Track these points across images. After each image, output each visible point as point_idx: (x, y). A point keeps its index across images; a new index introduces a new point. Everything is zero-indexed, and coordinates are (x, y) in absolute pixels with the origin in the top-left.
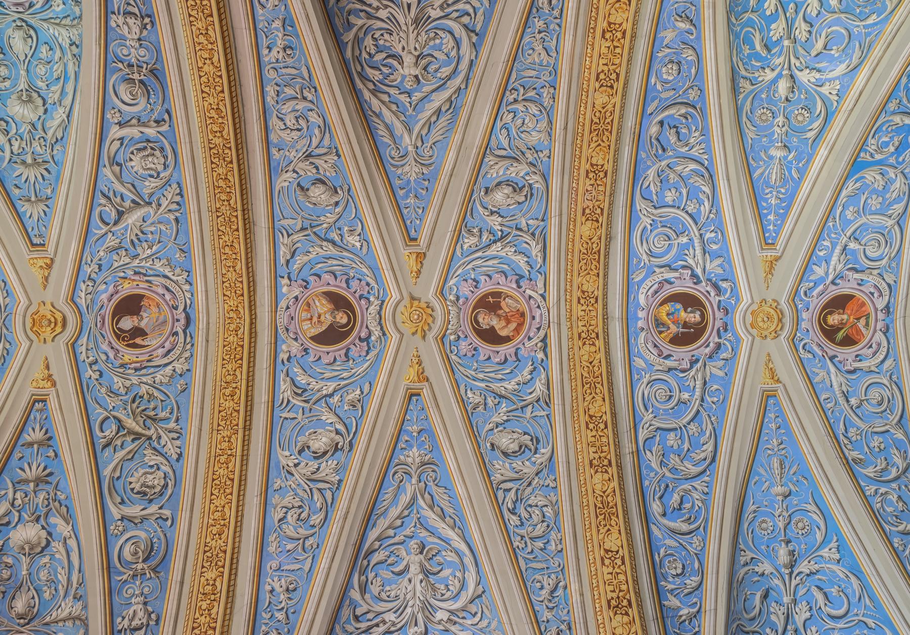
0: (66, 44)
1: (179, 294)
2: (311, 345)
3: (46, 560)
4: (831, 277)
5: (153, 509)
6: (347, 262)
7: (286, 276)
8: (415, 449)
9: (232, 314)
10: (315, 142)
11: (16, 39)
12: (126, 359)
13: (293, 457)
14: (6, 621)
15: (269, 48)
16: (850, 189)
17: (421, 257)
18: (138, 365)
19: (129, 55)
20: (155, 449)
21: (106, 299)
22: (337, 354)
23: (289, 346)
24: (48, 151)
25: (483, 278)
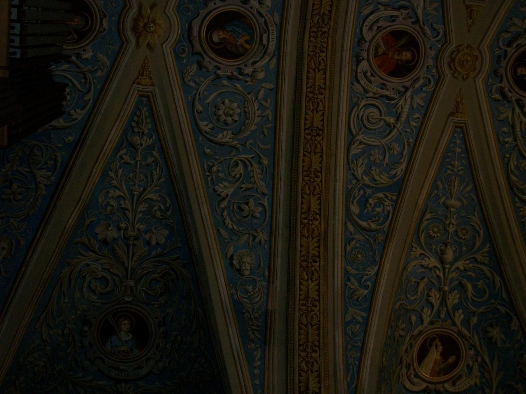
4: (409, 94)
16: (399, 169)
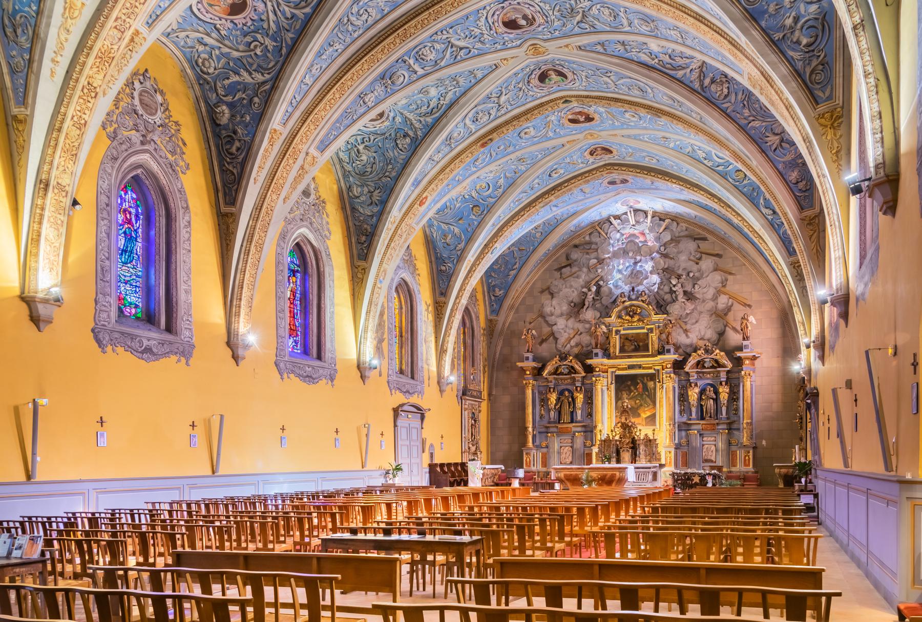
1: (494, 9)
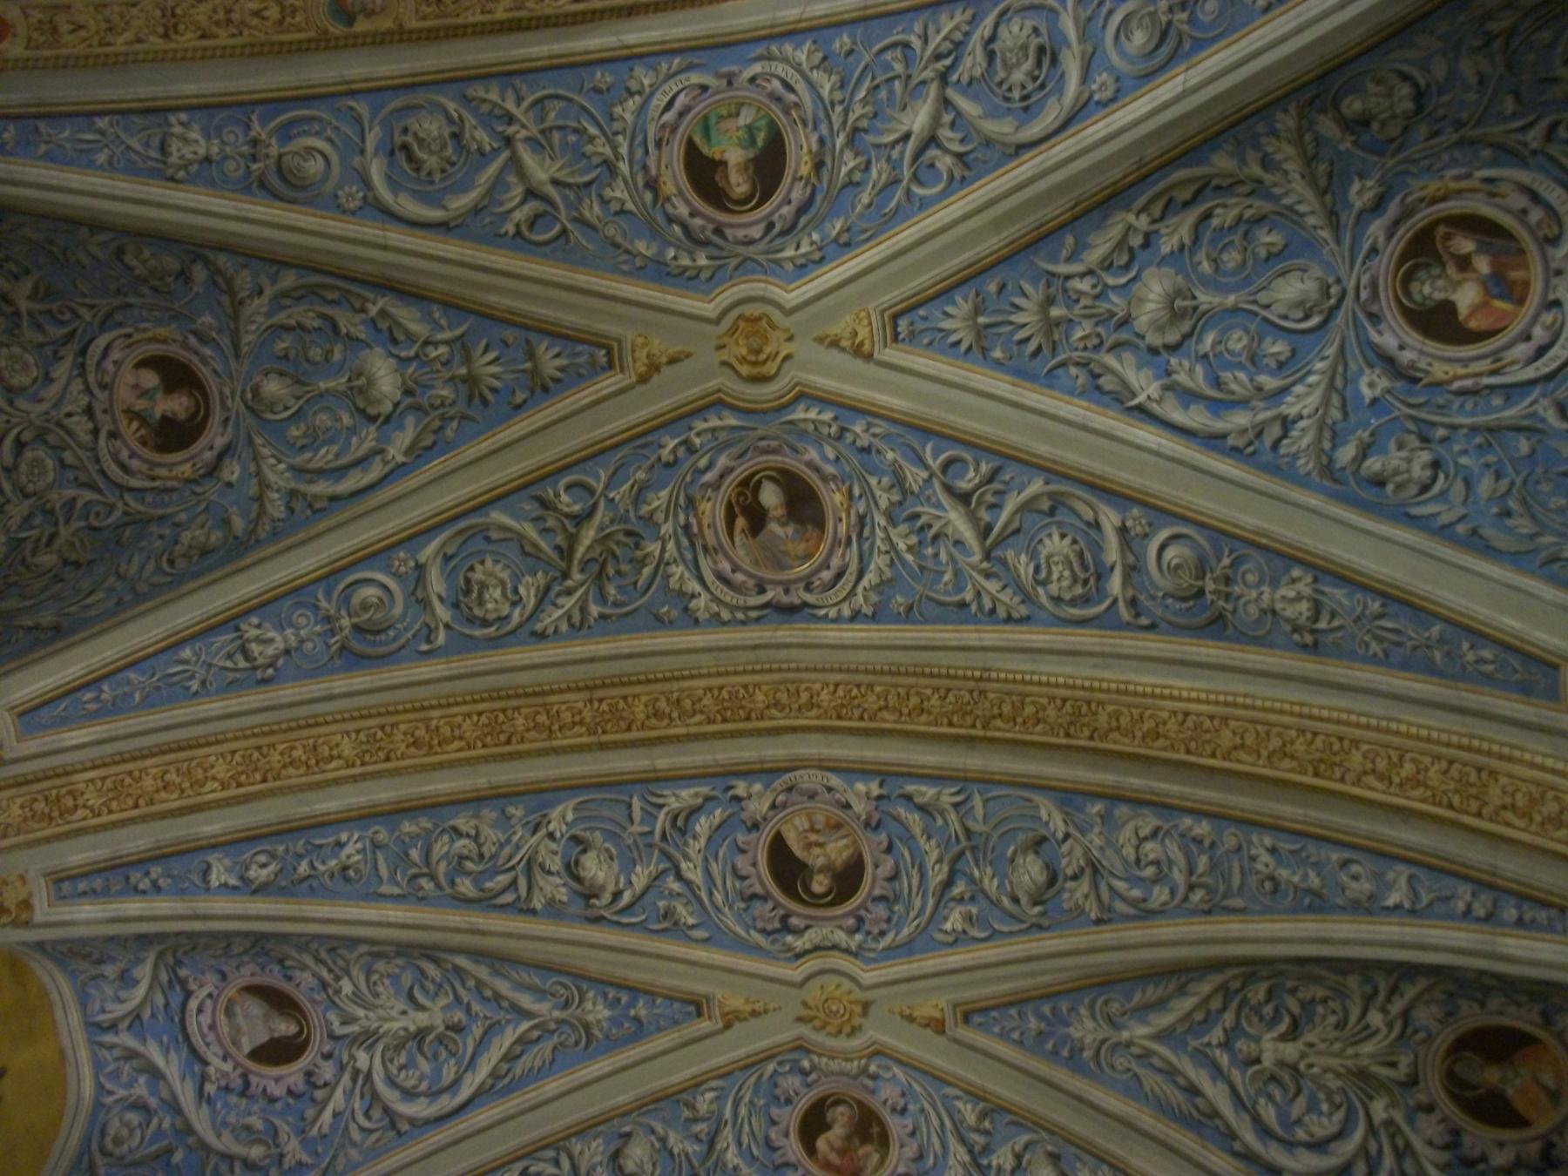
0: (1290, 407)
2: (766, 835)
3: (347, 420)
5: (443, 613)
6: (918, 903)
7: (884, 791)
8: (607, 1013)
9: (805, 696)
10: (1120, 885)
11: (1300, 285)
12: (705, 507)
13: (564, 828)
14: (245, 368)
15: (1273, 851)
17: (938, 1026)
18: (695, 530)
19: (1245, 584)
20: (548, 589)
21: (811, 458)
22: (754, 880)
23: (760, 795)
24: (1075, 355)
25: (909, 1122)
